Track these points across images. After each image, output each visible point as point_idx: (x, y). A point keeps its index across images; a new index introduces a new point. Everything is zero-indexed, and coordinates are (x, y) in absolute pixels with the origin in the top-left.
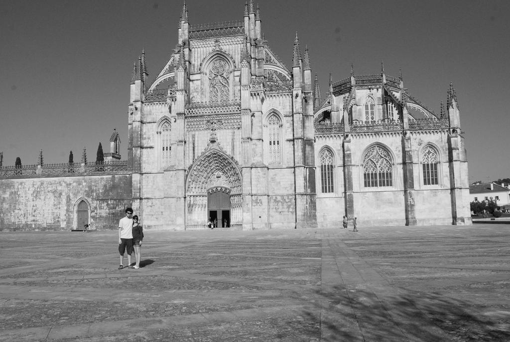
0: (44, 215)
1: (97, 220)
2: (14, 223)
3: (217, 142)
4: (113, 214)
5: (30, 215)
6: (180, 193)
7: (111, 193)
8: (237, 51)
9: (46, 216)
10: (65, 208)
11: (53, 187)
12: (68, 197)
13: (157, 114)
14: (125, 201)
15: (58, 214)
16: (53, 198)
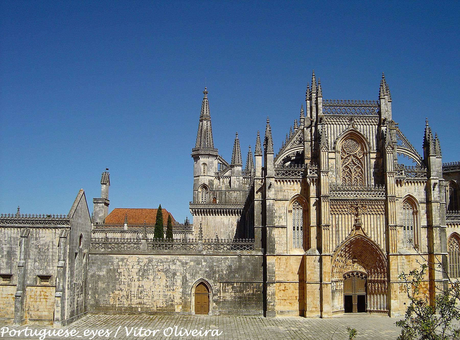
0: (153, 297)
1: (221, 305)
2: (113, 306)
3: (363, 227)
4: (240, 298)
5: (134, 297)
6: (327, 279)
7: (237, 275)
8: (371, 132)
9: (155, 298)
10: (181, 290)
11: (165, 266)
12: (184, 278)
13: (289, 191)
14: (255, 285)
15: (172, 296)
16: (164, 278)
